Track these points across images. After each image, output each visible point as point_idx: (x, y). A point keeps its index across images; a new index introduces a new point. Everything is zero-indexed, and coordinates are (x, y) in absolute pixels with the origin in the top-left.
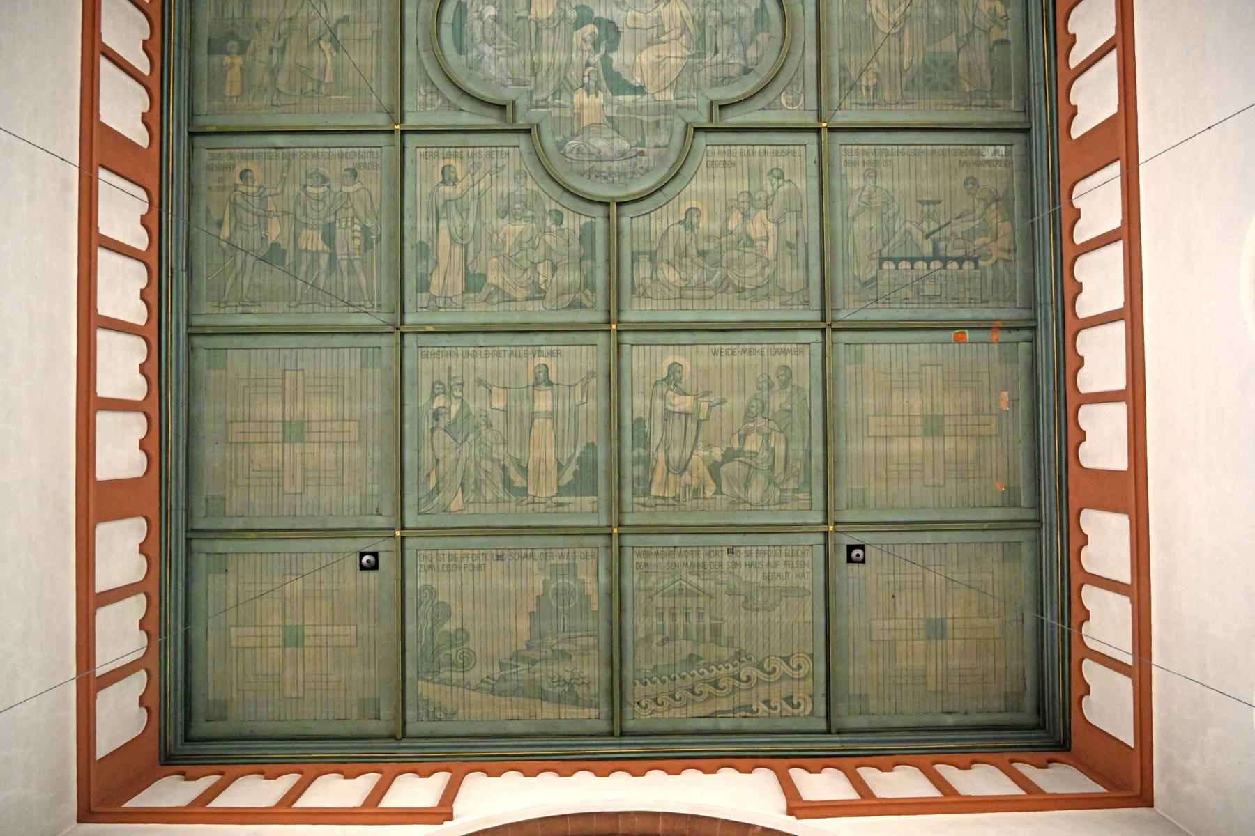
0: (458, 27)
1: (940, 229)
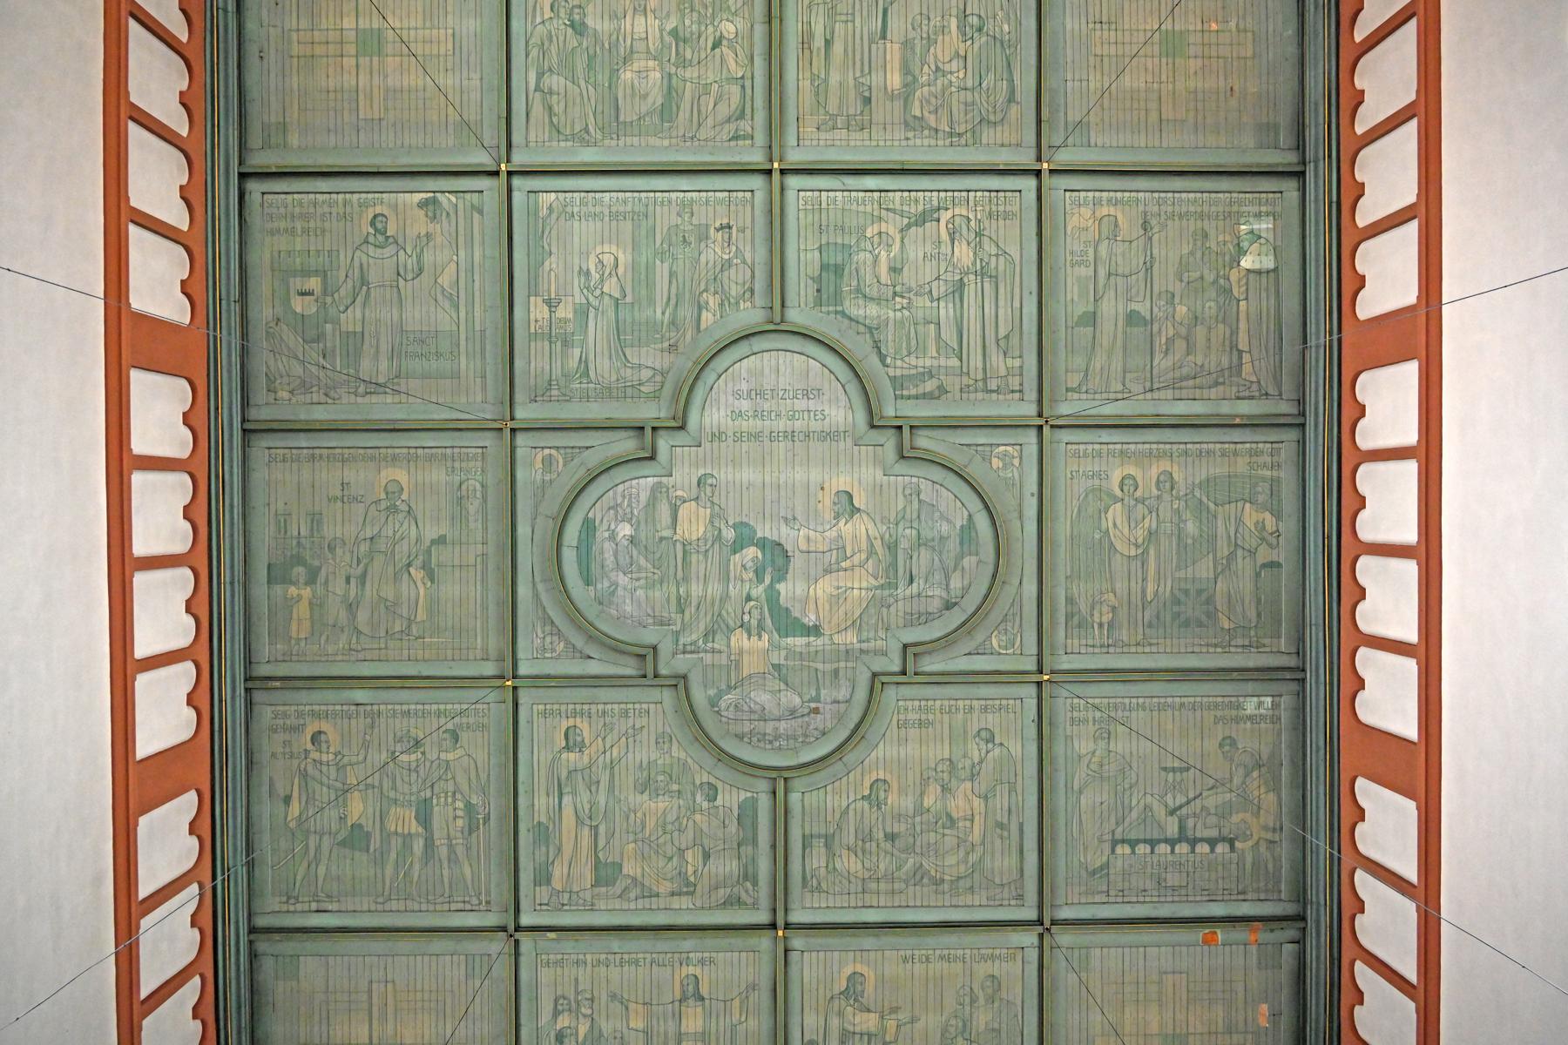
0: (584, 550)
1: (1188, 803)
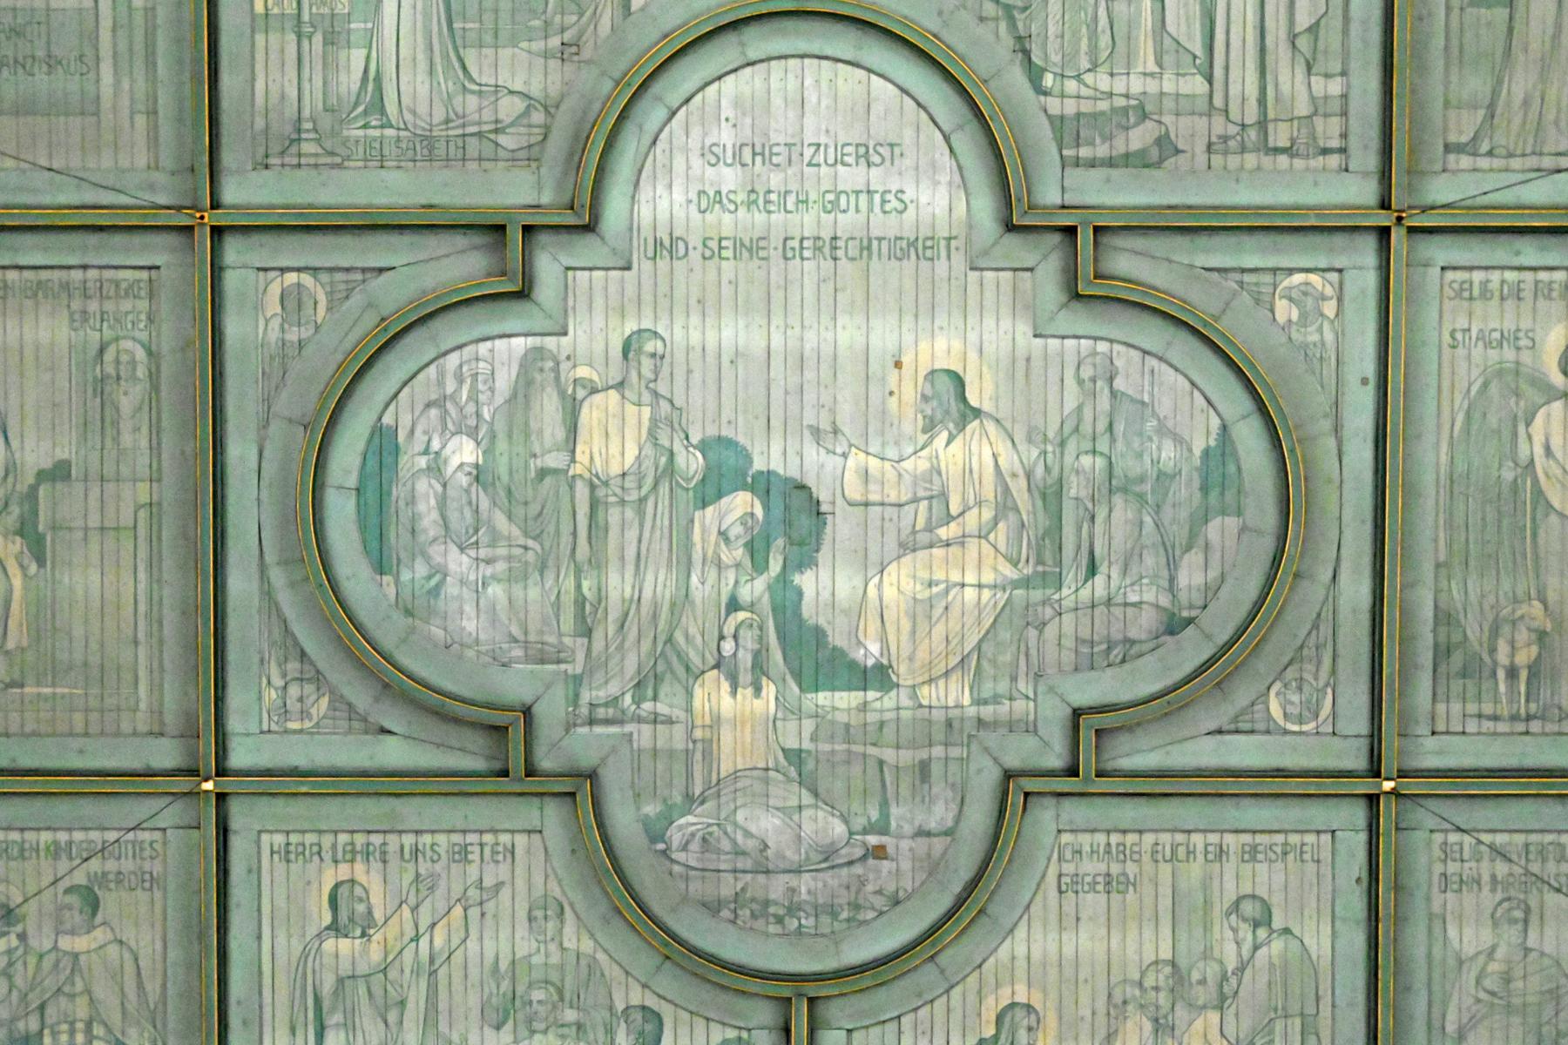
0: (371, 496)
